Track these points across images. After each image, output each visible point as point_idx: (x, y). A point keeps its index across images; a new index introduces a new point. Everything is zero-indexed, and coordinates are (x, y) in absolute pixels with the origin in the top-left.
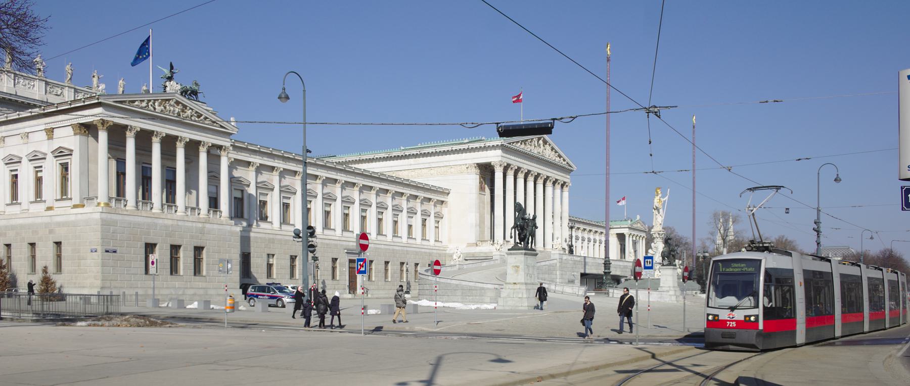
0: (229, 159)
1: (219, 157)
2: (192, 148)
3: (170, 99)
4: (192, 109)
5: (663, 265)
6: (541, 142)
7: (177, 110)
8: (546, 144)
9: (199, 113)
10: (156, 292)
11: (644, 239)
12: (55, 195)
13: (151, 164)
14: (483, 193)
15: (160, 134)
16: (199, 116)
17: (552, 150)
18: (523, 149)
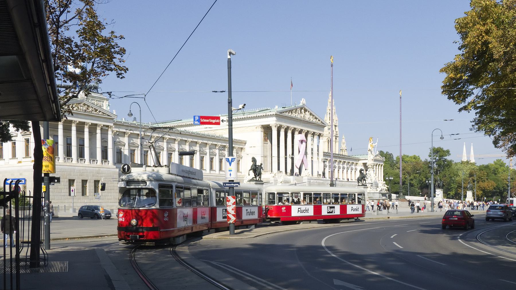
0: (113, 131)
1: (108, 130)
2: (93, 128)
3: (81, 103)
4: (92, 107)
5: (359, 186)
6: (303, 111)
7: (84, 108)
8: (306, 111)
9: (96, 109)
10: (75, 204)
11: (382, 166)
12: (22, 156)
13: (71, 137)
14: (266, 143)
15: (76, 122)
16: (96, 110)
17: (310, 115)
18: (290, 116)
